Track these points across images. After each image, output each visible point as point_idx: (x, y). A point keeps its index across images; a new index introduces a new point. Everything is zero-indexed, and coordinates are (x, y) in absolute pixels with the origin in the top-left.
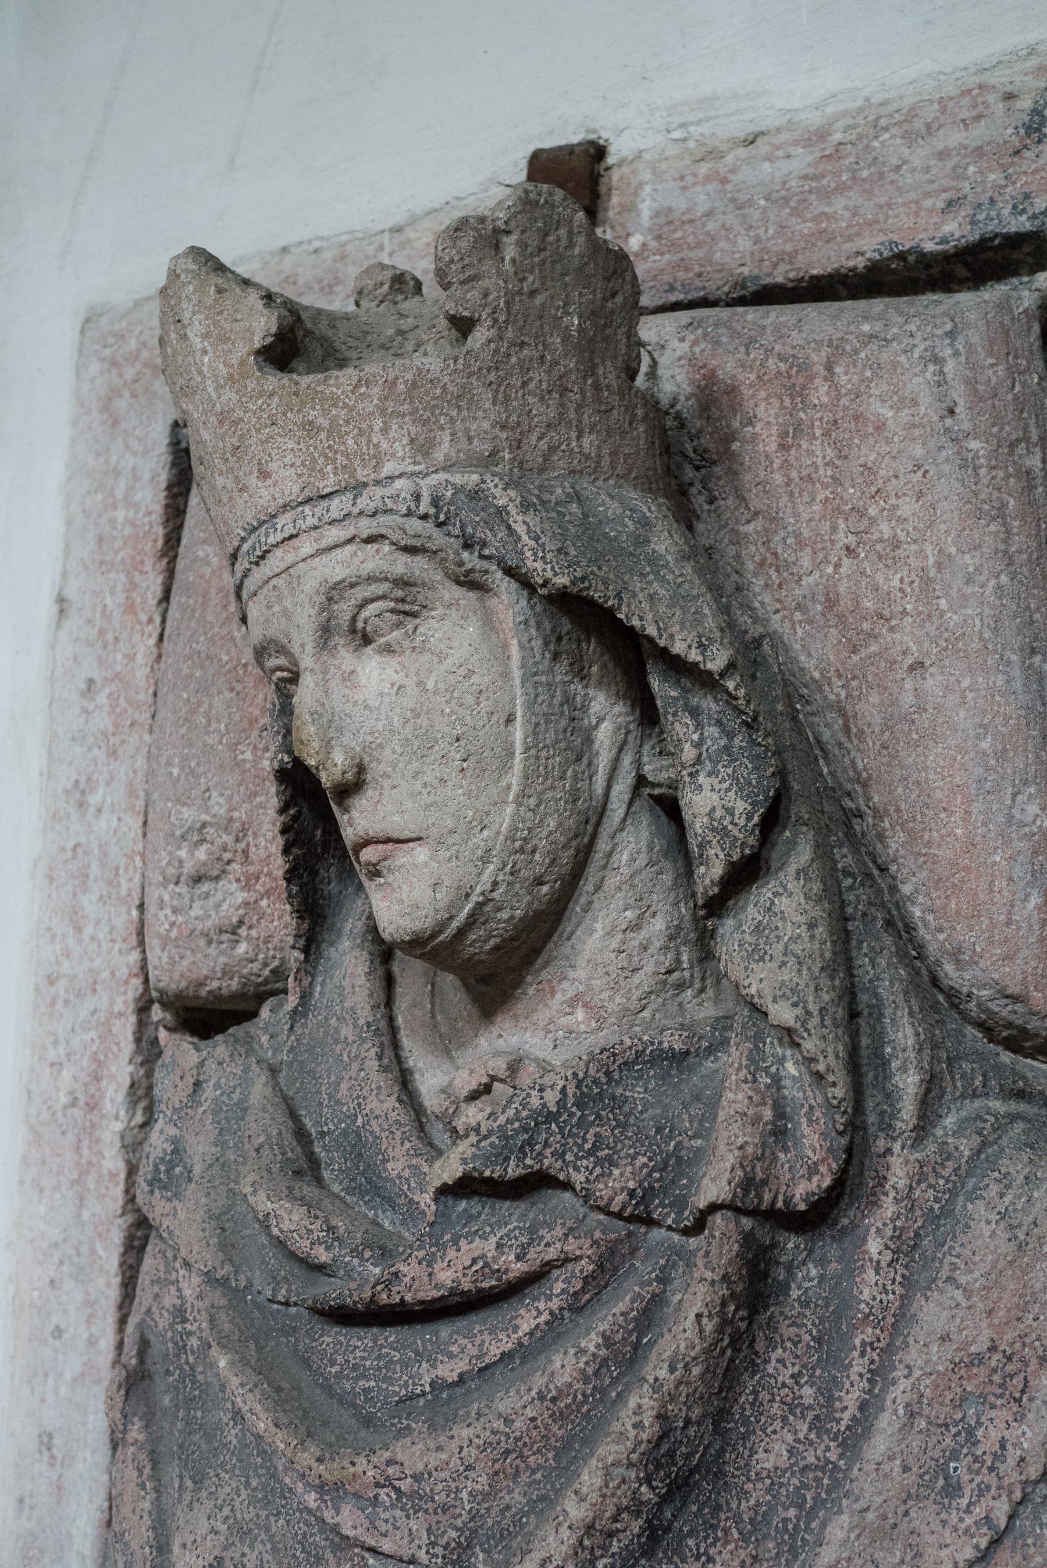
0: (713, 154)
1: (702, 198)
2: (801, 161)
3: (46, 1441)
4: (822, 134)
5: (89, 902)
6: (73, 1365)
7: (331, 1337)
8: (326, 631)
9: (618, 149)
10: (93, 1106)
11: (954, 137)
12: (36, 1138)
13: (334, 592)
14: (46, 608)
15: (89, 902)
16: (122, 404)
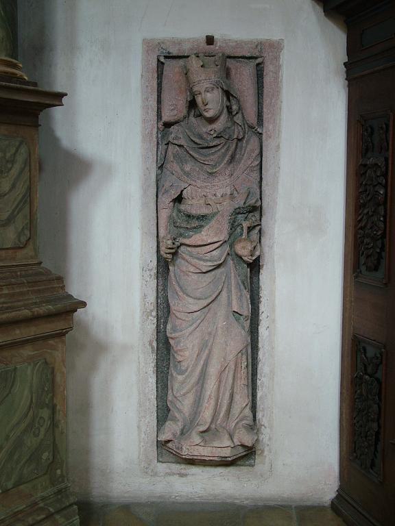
0: (225, 40)
1: (224, 45)
2: (234, 44)
3: (147, 168)
4: (236, 42)
5: (149, 111)
6: (151, 160)
7: (201, 150)
8: (205, 91)
9: (215, 37)
10: (152, 133)
11: (249, 46)
12: (143, 137)
13: (207, 88)
14: (140, 76)
15: (149, 111)
16: (149, 52)
